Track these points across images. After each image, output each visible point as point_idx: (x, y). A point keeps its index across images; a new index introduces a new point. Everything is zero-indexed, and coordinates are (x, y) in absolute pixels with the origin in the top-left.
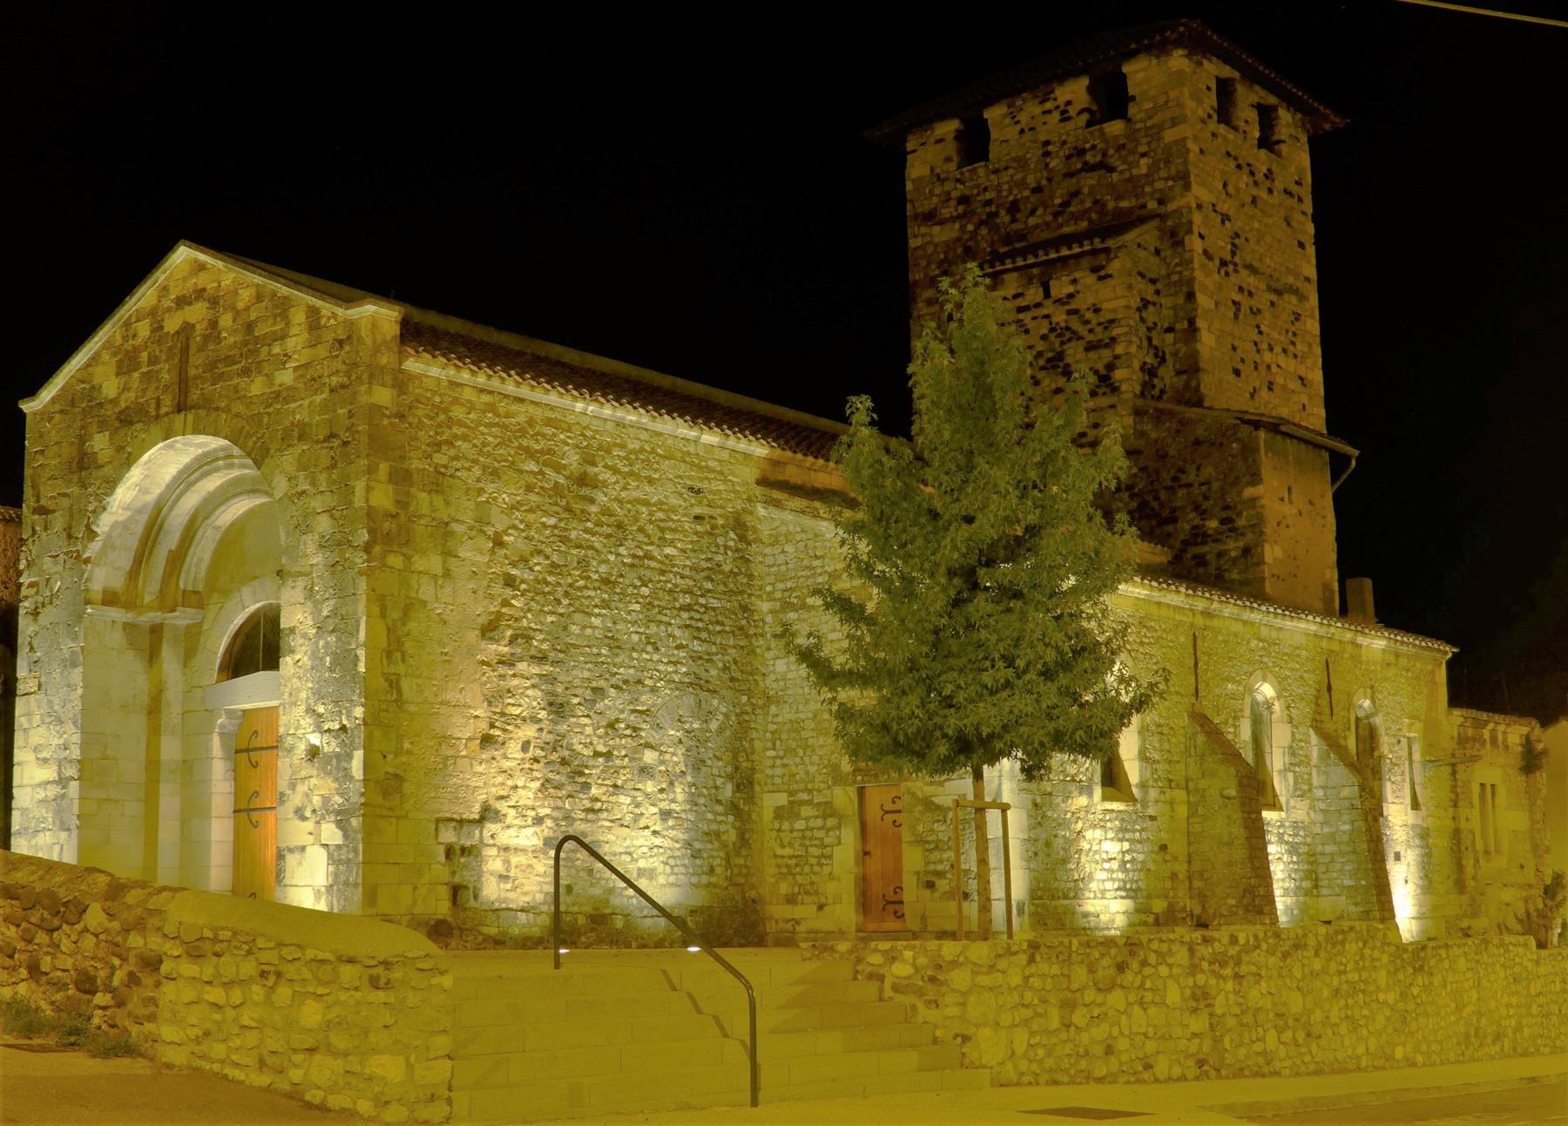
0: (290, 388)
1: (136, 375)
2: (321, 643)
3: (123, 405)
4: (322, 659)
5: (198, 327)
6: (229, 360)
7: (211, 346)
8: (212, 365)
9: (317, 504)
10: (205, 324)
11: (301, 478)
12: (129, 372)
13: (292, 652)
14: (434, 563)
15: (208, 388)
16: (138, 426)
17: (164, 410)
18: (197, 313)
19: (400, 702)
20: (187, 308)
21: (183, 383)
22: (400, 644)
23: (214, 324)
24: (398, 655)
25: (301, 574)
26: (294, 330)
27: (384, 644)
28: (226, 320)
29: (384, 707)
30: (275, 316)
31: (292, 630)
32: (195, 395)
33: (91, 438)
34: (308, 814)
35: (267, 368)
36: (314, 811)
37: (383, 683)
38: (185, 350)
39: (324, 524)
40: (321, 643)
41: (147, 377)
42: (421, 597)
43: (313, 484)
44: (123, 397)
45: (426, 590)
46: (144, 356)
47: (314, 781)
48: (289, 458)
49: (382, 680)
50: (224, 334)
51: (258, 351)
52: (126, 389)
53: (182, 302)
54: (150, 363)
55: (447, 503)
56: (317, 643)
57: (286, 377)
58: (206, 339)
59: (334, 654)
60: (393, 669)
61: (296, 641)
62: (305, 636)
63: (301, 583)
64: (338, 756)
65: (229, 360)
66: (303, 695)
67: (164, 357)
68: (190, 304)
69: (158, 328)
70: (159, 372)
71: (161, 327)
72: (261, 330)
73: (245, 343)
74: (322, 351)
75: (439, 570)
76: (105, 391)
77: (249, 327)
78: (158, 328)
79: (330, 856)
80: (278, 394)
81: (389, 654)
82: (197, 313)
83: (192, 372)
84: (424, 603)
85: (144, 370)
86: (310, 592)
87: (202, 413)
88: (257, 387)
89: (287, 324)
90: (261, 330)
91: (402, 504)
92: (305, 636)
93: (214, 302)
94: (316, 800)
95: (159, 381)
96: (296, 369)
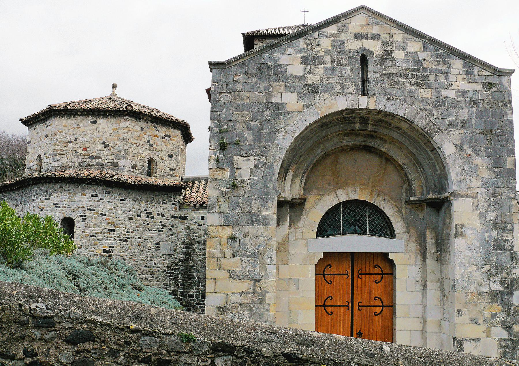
0: (452, 100)
17: (347, 91)
20: (364, 41)
21: (364, 81)
34: (481, 321)
36: (485, 320)
40: (487, 235)
43: (475, 151)
48: (456, 137)
51: (427, 77)
57: (450, 94)
62: (474, 229)
64: (502, 293)
68: (366, 38)
73: (414, 70)
79: (500, 344)
82: (370, 44)
83: (371, 75)
85: (328, 65)
88: (427, 94)
92: (474, 229)
94: (487, 315)
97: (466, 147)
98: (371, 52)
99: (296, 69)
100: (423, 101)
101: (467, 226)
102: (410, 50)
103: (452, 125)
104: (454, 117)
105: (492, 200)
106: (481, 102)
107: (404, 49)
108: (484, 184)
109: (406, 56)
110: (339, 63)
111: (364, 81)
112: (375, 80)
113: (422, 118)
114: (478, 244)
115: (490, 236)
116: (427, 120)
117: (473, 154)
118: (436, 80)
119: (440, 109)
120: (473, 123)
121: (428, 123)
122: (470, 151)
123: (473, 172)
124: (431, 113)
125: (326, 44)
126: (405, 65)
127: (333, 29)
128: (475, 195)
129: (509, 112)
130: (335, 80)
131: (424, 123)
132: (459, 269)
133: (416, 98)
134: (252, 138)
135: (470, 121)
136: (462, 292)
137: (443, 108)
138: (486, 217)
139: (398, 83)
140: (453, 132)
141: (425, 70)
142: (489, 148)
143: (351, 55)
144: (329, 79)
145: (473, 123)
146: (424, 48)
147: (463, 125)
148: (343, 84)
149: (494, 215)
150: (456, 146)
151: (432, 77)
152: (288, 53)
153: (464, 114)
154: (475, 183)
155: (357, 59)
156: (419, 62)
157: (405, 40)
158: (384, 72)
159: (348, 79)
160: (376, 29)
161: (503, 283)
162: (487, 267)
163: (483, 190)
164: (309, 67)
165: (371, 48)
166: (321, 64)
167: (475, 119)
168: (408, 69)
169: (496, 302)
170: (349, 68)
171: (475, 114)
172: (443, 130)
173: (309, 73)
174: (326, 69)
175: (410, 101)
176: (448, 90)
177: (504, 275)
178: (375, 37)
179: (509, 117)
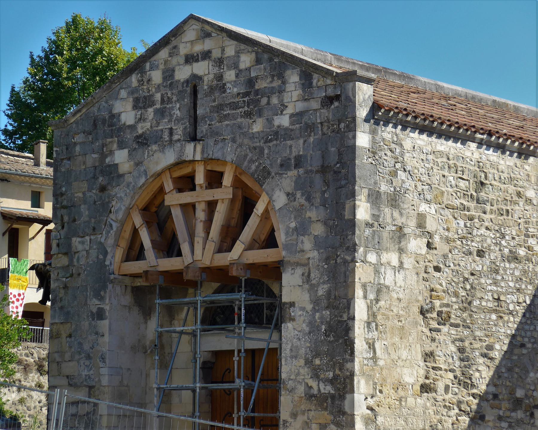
0: (286, 129)
1: (151, 110)
2: (317, 315)
3: (140, 131)
4: (318, 329)
5: (206, 79)
6: (234, 106)
7: (217, 94)
8: (220, 108)
9: (312, 214)
10: (211, 76)
11: (299, 195)
12: (145, 108)
13: (292, 319)
14: (393, 258)
15: (216, 124)
16: (154, 147)
17: (176, 137)
18: (201, 68)
19: (375, 358)
20: (195, 65)
21: (195, 120)
22: (374, 315)
23: (220, 77)
24: (374, 324)
25: (298, 264)
26: (290, 87)
27: (365, 318)
28: (230, 75)
29: (366, 362)
30: (273, 76)
31: (292, 304)
32: (203, 129)
33: (111, 153)
35: (267, 113)
37: (366, 347)
38: (195, 92)
39: (318, 229)
41: (161, 113)
42: (387, 283)
43: (309, 199)
44: (140, 125)
45: (389, 278)
46: (158, 97)
47: (312, 413)
48: (288, 181)
49: (364, 343)
50: (228, 85)
51: (259, 101)
52: (141, 119)
53: (190, 59)
54: (163, 101)
55: (401, 214)
56: (313, 316)
57: (284, 121)
58: (212, 89)
59: (329, 324)
60: (370, 335)
61: (295, 312)
63: (299, 271)
64: (333, 397)
65: (234, 106)
66: (302, 351)
67: (175, 98)
68: (197, 61)
69: (169, 74)
70: (172, 108)
71: (172, 76)
72: (261, 85)
73: (247, 94)
74: (315, 104)
75: (395, 262)
76: (123, 118)
77: (251, 82)
78: (169, 74)
80: (276, 133)
81: (369, 324)
83: (200, 112)
84: (387, 287)
85: (158, 106)
86: (307, 278)
87: (211, 142)
88: (258, 126)
89: (284, 83)
90: (261, 85)
91: (376, 217)
92: (303, 309)
93: (220, 62)
95: (171, 116)
96: (292, 116)
97: (299, 195)
98: (200, 78)
99: (128, 116)
100: (253, 137)
101: (296, 305)
102: (242, 66)
103: (285, 165)
104: (286, 154)
105: (326, 266)
106: (319, 126)
107: (235, 66)
108: (318, 244)
109: (237, 76)
110: (170, 100)
111: (195, 120)
112: (204, 118)
113: (252, 161)
114: (307, 329)
115: (321, 318)
116: (257, 164)
117: (306, 204)
118: (268, 103)
119: (271, 144)
120: (309, 159)
121: (257, 167)
122: (303, 201)
123: (302, 229)
124: (262, 150)
125: (157, 76)
126: (235, 90)
127: (163, 54)
128: (306, 262)
129: (351, 135)
130: (164, 125)
131: (253, 167)
132: (286, 365)
133: (244, 134)
134: (87, 213)
135: (305, 156)
136: (288, 397)
137: (275, 142)
138: (317, 291)
139: (226, 117)
140: (284, 176)
141: (257, 92)
142: (325, 192)
143: (180, 88)
144: (158, 124)
145: (309, 159)
146: (258, 61)
147: (299, 162)
148: (171, 129)
149: (326, 286)
150: (288, 194)
151: (264, 101)
152: (121, 96)
153: (297, 147)
154: (307, 244)
155: (186, 91)
156: (251, 82)
157: (238, 53)
158: (213, 104)
159: (178, 120)
160: (207, 45)
161: (332, 382)
162: (317, 362)
163: (315, 254)
164: (139, 113)
165: (200, 73)
166: (151, 106)
167: (311, 152)
168: (239, 94)
169: (326, 409)
170: (178, 106)
171: (312, 146)
172: (273, 174)
173: (140, 119)
174: (156, 112)
175: (239, 141)
176: (282, 116)
177: (337, 372)
178: (206, 55)
179: (350, 143)
